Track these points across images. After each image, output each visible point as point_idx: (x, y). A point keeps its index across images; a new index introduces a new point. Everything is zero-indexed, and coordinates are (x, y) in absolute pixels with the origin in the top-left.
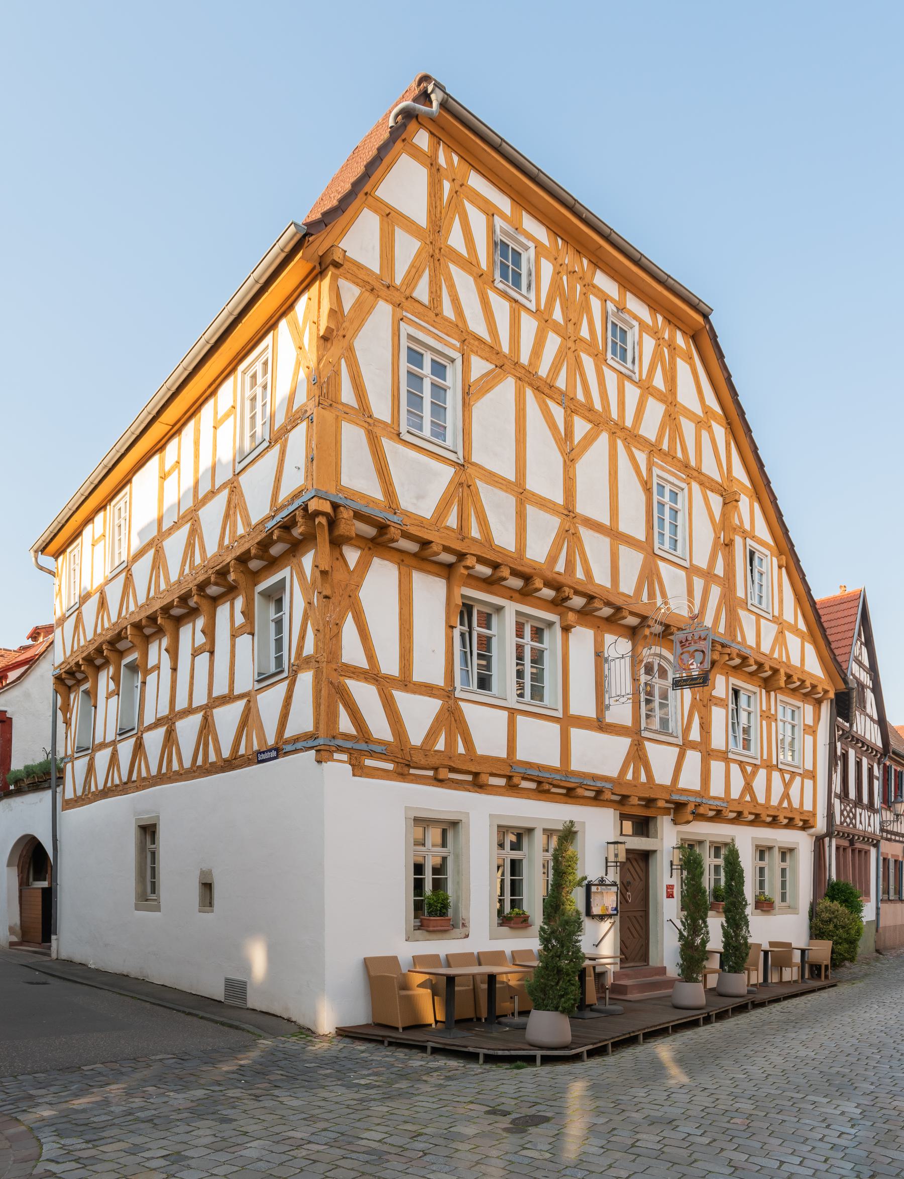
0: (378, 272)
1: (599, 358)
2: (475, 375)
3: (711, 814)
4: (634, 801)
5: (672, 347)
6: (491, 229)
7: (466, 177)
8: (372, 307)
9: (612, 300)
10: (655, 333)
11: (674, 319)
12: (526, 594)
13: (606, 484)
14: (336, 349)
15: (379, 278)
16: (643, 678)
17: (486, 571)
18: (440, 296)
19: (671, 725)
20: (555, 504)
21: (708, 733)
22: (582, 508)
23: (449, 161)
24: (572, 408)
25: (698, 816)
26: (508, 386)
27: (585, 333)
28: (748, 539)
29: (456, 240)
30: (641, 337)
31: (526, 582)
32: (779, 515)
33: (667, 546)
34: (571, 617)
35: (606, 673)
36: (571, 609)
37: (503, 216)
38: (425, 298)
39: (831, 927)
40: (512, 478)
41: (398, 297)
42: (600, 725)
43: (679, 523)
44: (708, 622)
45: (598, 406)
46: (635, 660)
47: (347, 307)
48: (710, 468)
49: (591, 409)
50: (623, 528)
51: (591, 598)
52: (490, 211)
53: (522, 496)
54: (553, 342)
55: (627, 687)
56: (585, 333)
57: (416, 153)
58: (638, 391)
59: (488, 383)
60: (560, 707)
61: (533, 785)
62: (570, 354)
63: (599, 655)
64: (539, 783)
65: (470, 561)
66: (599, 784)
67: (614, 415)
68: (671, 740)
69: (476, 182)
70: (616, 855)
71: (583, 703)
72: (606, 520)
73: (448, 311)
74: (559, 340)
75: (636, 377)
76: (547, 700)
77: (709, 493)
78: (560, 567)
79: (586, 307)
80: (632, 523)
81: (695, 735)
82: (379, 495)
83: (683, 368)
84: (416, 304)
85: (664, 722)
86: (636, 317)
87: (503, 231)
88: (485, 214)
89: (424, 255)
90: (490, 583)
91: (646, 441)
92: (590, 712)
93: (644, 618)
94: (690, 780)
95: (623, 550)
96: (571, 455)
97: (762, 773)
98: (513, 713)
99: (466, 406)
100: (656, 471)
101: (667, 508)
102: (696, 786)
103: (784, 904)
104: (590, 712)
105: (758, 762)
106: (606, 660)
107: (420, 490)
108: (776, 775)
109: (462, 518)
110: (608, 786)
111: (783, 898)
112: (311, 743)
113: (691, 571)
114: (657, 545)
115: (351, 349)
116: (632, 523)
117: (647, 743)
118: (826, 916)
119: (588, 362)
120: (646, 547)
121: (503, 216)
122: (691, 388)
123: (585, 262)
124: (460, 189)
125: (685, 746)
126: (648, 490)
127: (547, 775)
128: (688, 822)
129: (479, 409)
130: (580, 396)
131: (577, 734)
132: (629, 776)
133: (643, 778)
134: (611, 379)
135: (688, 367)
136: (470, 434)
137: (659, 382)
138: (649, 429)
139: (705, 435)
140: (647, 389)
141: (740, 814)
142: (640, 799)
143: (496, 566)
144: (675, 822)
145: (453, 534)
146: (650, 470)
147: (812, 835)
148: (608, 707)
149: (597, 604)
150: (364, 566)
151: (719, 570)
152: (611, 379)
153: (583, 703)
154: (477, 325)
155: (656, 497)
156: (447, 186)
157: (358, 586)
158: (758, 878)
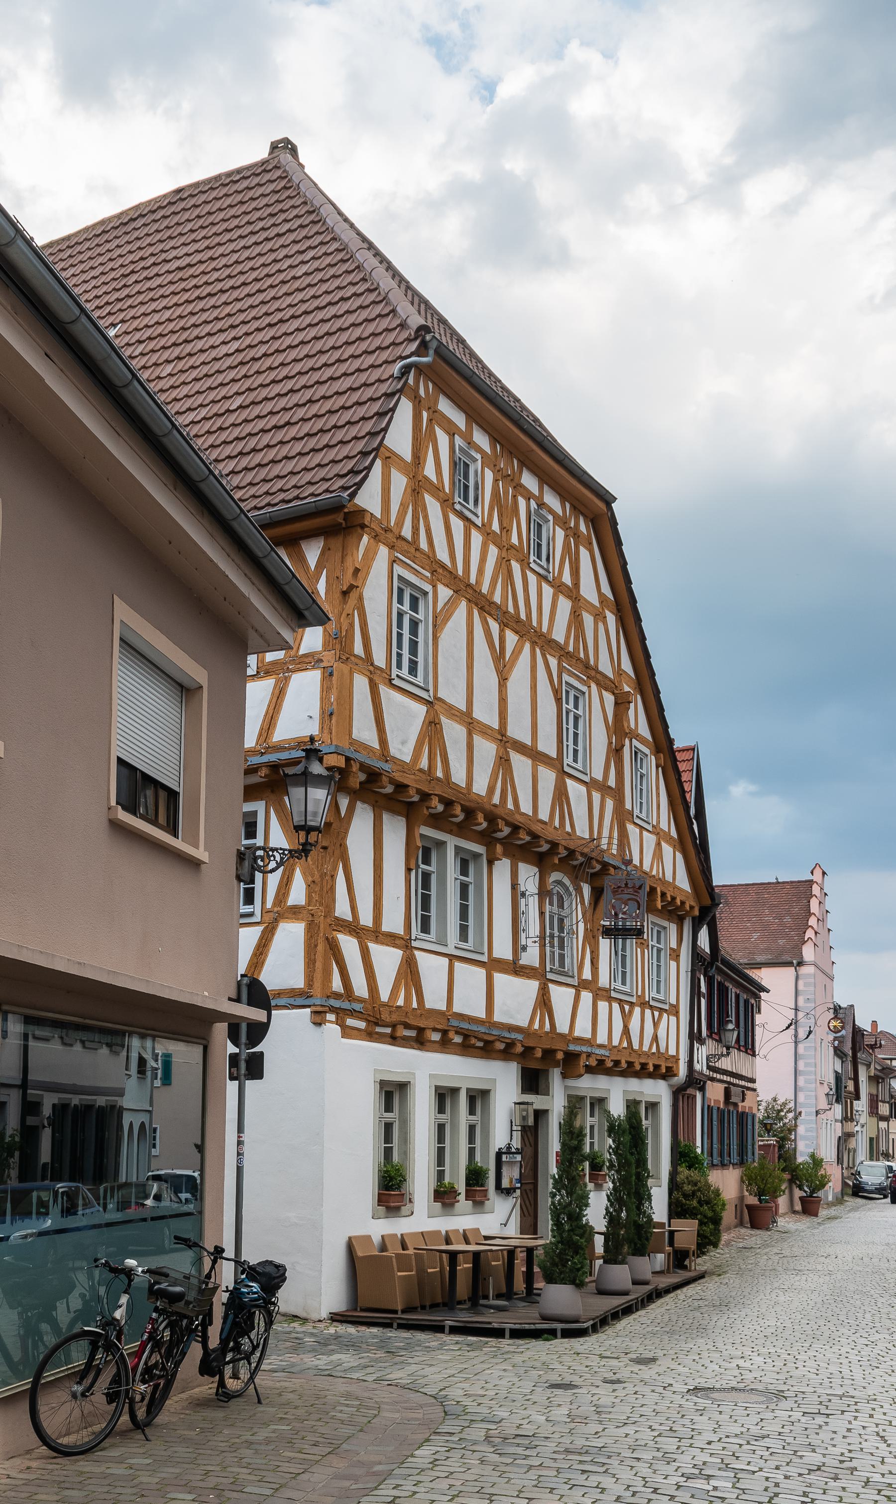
28: (633, 740)
32: (661, 709)
35: (523, 908)
42: (516, 969)
68: (569, 980)
81: (587, 974)
92: (508, 955)
97: (637, 1010)
104: (508, 955)
105: (634, 1000)
106: (523, 895)
108: (648, 1012)
151: (612, 783)
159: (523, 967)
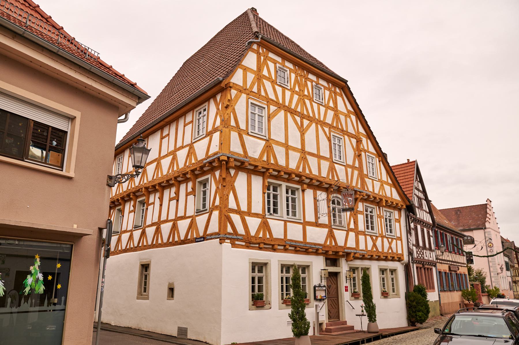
0: (242, 85)
1: (311, 100)
2: (271, 111)
3: (361, 256)
4: (331, 253)
5: (335, 93)
6: (276, 67)
7: (268, 54)
8: (240, 96)
9: (314, 82)
10: (329, 89)
11: (335, 85)
12: (288, 180)
13: (315, 140)
14: (230, 110)
15: (242, 87)
16: (331, 206)
17: (276, 173)
18: (260, 90)
19: (343, 223)
20: (298, 149)
21: (357, 225)
22: (307, 149)
23: (263, 51)
24: (303, 117)
25: (356, 258)
26: (282, 113)
27: (306, 93)
29: (265, 72)
30: (324, 91)
31: (288, 176)
33: (337, 159)
34: (305, 186)
36: (305, 183)
37: (279, 63)
38: (256, 91)
39: (414, 303)
40: (284, 142)
41: (247, 92)
42: (316, 224)
43: (341, 150)
44: (354, 184)
45: (311, 115)
46: (328, 200)
47: (233, 97)
48: (351, 130)
49: (309, 117)
50: (321, 154)
51: (311, 179)
52: (275, 62)
53: (287, 147)
54: (296, 97)
55: (326, 211)
57: (253, 51)
58: (324, 108)
59: (275, 113)
60: (302, 219)
61: (293, 248)
62: (301, 100)
63: (316, 200)
64: (296, 247)
65: (271, 171)
66: (317, 247)
67: (317, 117)
68: (343, 228)
69: (271, 55)
70: (325, 275)
71: (310, 217)
72: (315, 152)
73: (263, 93)
74: (297, 96)
75: (324, 104)
76: (297, 217)
77: (351, 139)
78: (301, 170)
79: (306, 85)
80: (325, 152)
82: (242, 153)
83: (339, 99)
84: (254, 94)
85: (340, 222)
86: (322, 86)
87: (279, 67)
88: (273, 64)
89: (256, 78)
90: (276, 177)
91: (328, 124)
92: (313, 220)
93: (331, 185)
94: (351, 243)
95: (323, 162)
96: (303, 131)
98: (285, 221)
99: (269, 121)
100: (332, 134)
101: (337, 145)
102: (354, 246)
103: (394, 293)
104: (313, 220)
106: (318, 201)
107: (255, 149)
109: (268, 157)
110: (321, 247)
111: (394, 291)
112: (217, 236)
113: (347, 166)
114: (334, 159)
115: (234, 109)
116: (325, 152)
117: (334, 230)
118: (412, 298)
119: (307, 102)
120: (330, 160)
121: (279, 63)
122: (342, 105)
123: (305, 72)
124: (267, 58)
125: (349, 230)
126: (330, 140)
127: (298, 244)
128: (351, 260)
129: (273, 121)
130: (305, 113)
131: (308, 228)
132: (328, 243)
133: (333, 244)
134: (315, 106)
135: (341, 98)
136: (270, 130)
137: (331, 104)
138: (329, 120)
140: (327, 107)
141: (372, 256)
142: (333, 252)
143: (279, 172)
144: (347, 261)
145: (265, 163)
146: (330, 134)
147: (403, 264)
148: (319, 218)
149: (314, 181)
150: (236, 174)
152: (315, 106)
153: (310, 217)
154: (272, 96)
155: (332, 142)
156: (262, 58)
157: (234, 181)
158: (382, 283)
159: (320, 224)
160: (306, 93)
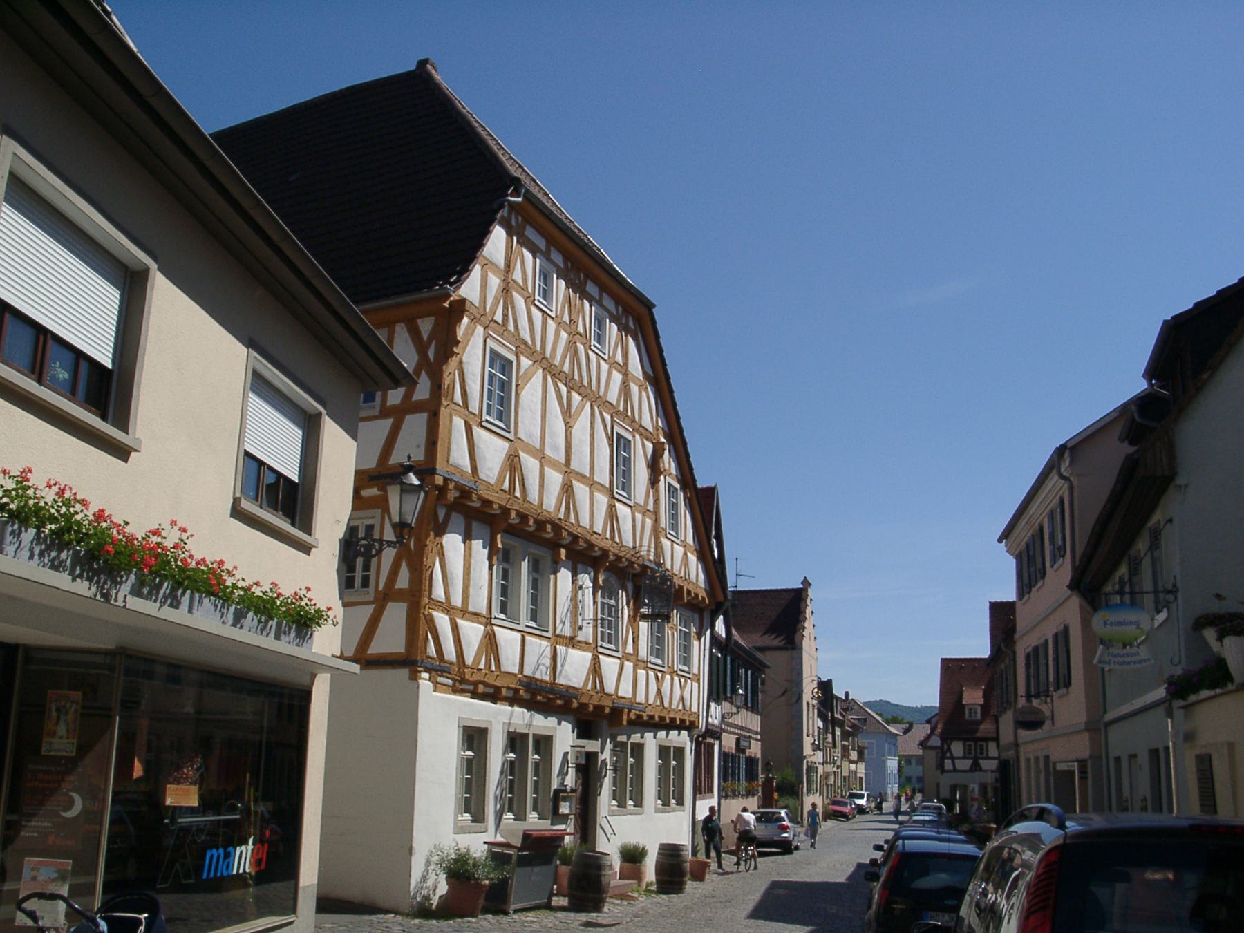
29: (517, 275)
56: (580, 329)
137: (619, 358)
138: (613, 396)
139: (644, 394)
140: (613, 364)
160: (580, 329)
